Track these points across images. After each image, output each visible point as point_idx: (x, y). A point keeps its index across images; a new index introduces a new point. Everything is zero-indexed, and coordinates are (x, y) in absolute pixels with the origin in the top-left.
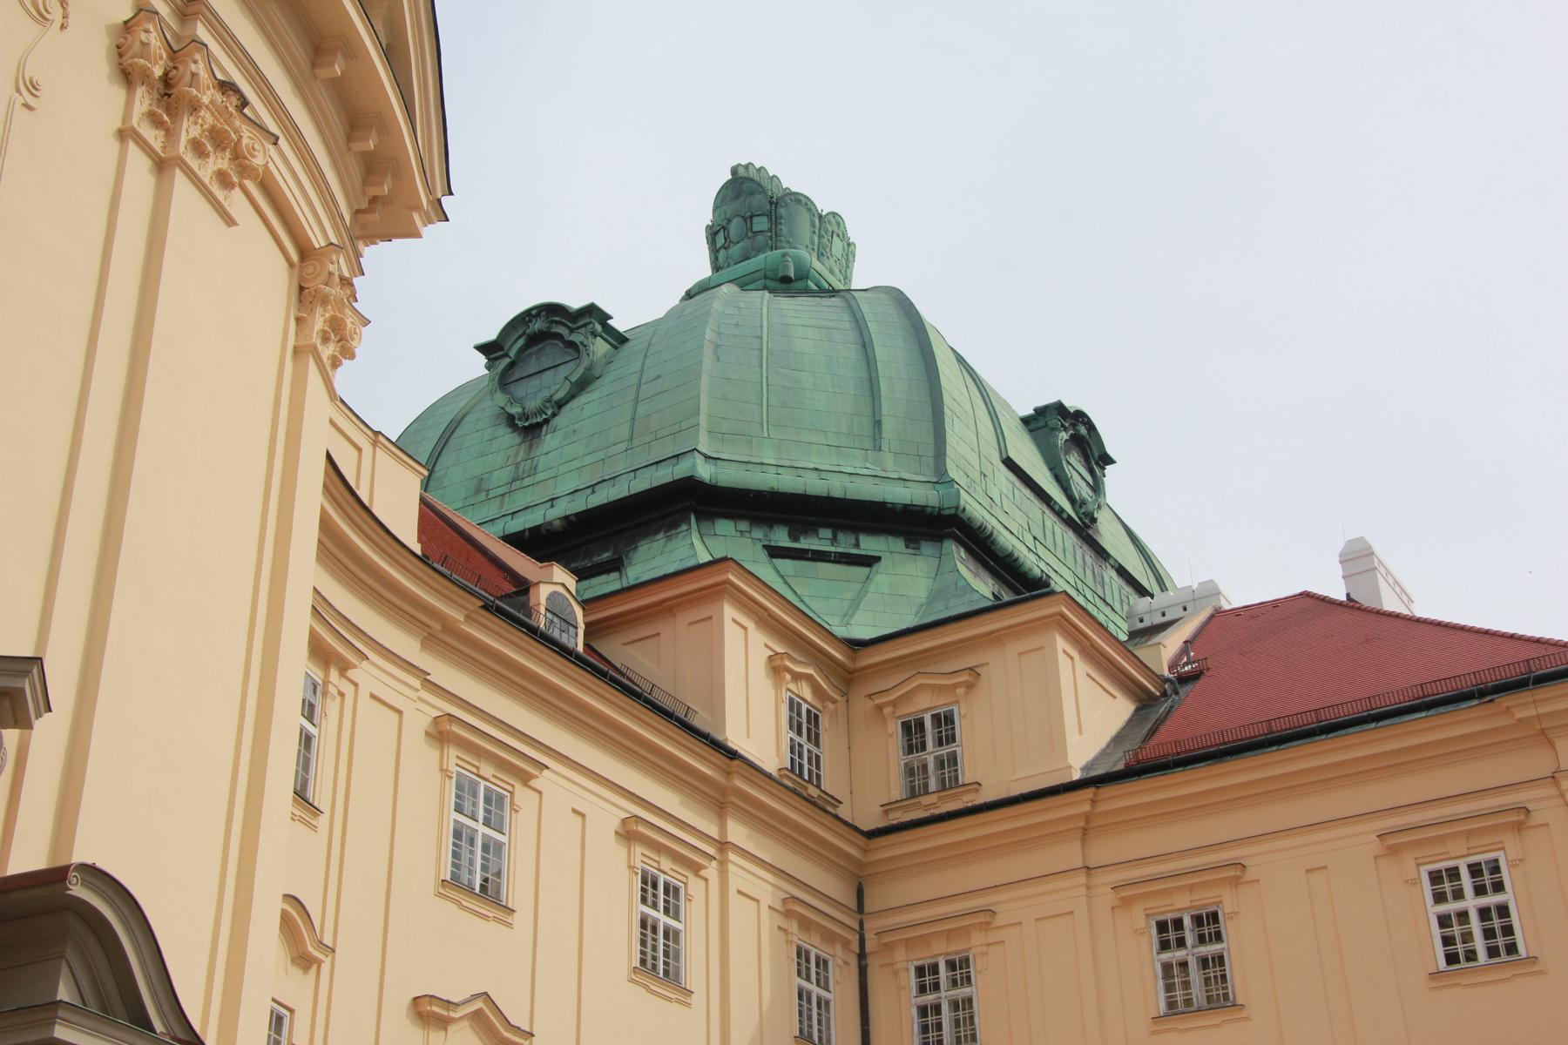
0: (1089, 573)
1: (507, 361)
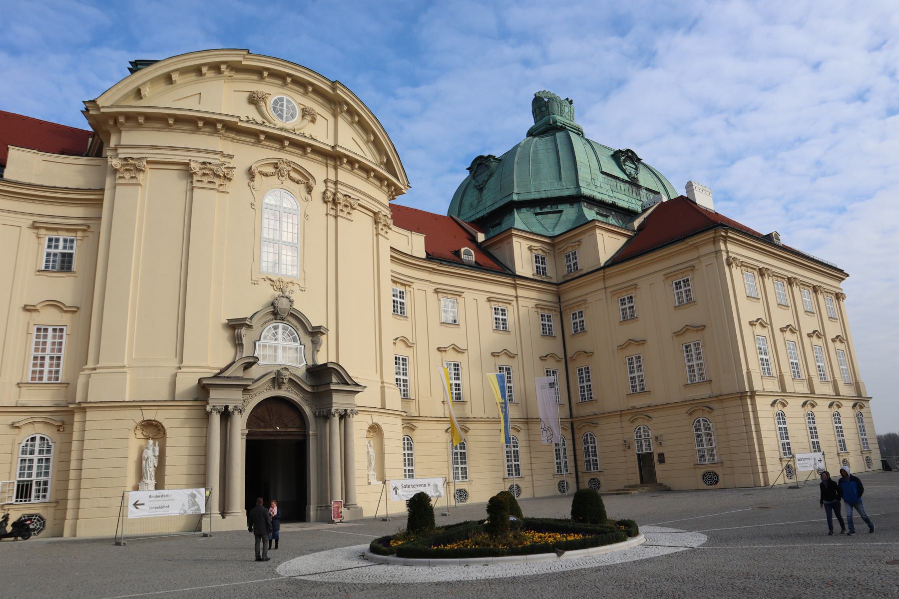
0: (634, 194)
1: (474, 172)
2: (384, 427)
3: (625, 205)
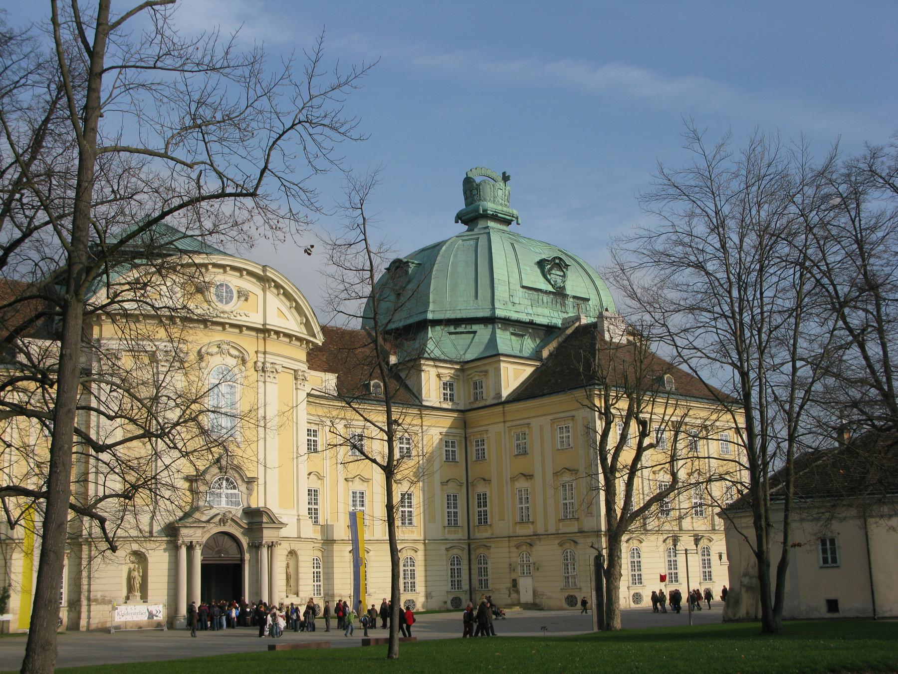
0: (558, 305)
2: (299, 553)
3: (544, 321)
